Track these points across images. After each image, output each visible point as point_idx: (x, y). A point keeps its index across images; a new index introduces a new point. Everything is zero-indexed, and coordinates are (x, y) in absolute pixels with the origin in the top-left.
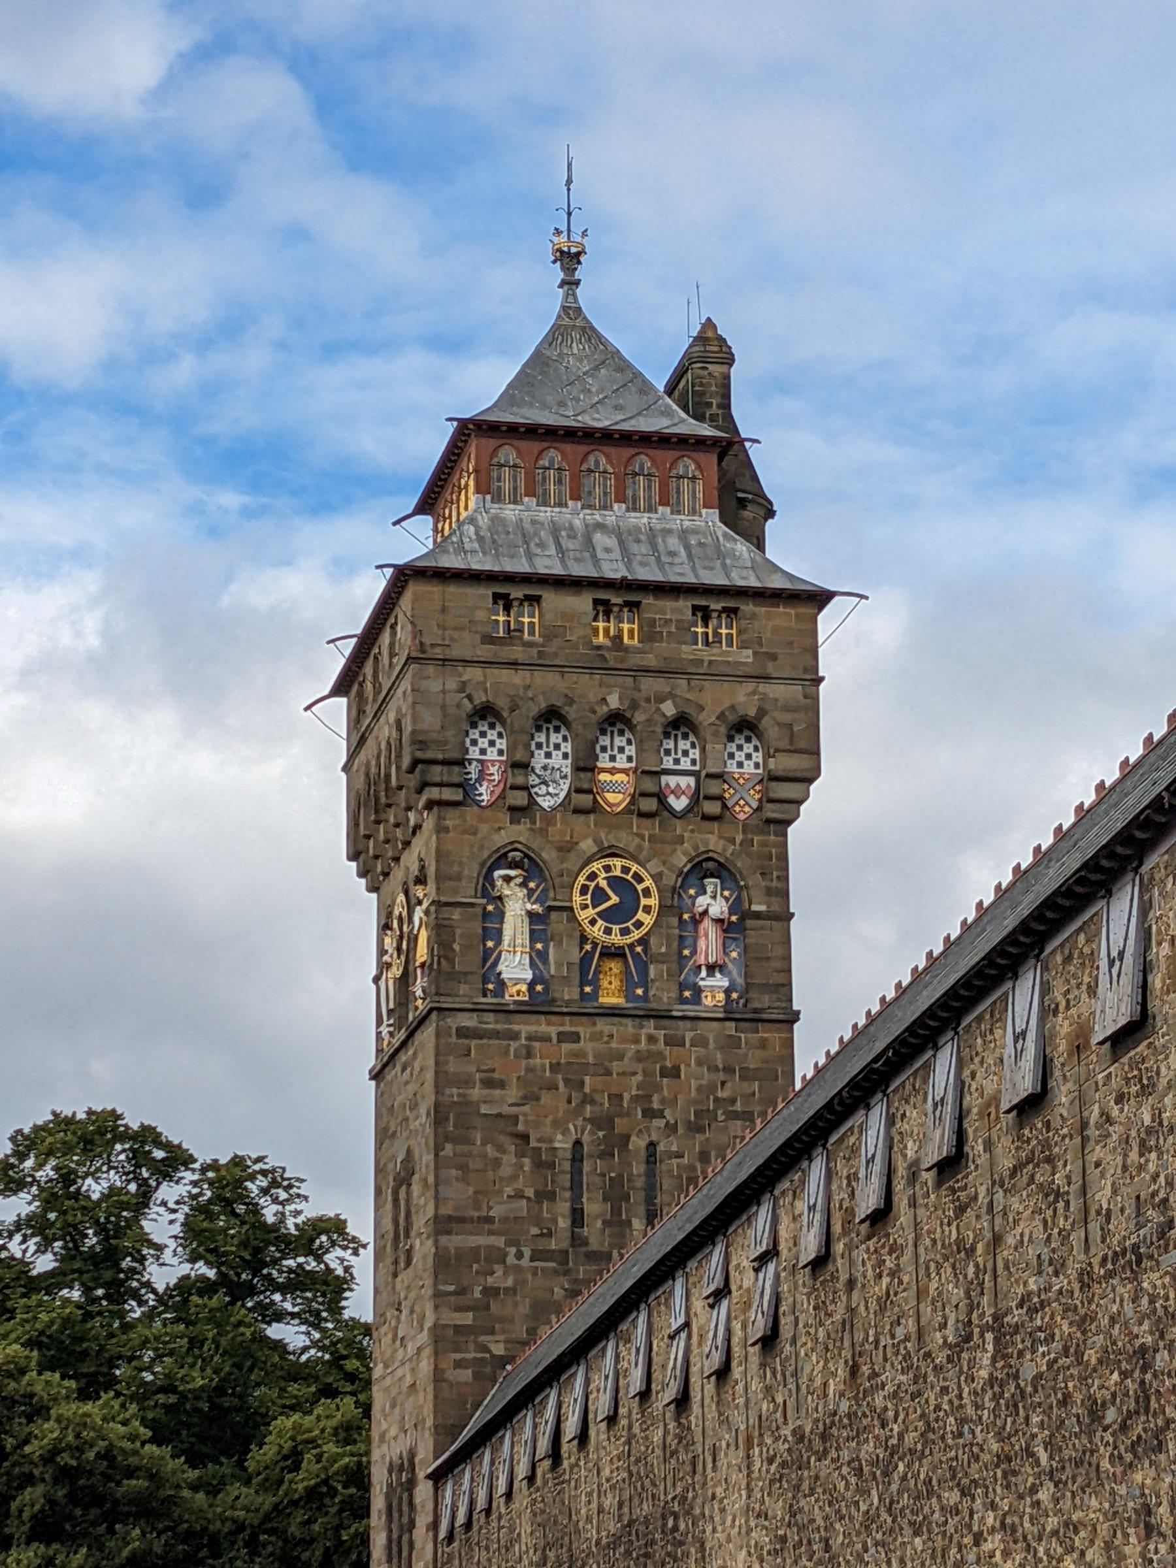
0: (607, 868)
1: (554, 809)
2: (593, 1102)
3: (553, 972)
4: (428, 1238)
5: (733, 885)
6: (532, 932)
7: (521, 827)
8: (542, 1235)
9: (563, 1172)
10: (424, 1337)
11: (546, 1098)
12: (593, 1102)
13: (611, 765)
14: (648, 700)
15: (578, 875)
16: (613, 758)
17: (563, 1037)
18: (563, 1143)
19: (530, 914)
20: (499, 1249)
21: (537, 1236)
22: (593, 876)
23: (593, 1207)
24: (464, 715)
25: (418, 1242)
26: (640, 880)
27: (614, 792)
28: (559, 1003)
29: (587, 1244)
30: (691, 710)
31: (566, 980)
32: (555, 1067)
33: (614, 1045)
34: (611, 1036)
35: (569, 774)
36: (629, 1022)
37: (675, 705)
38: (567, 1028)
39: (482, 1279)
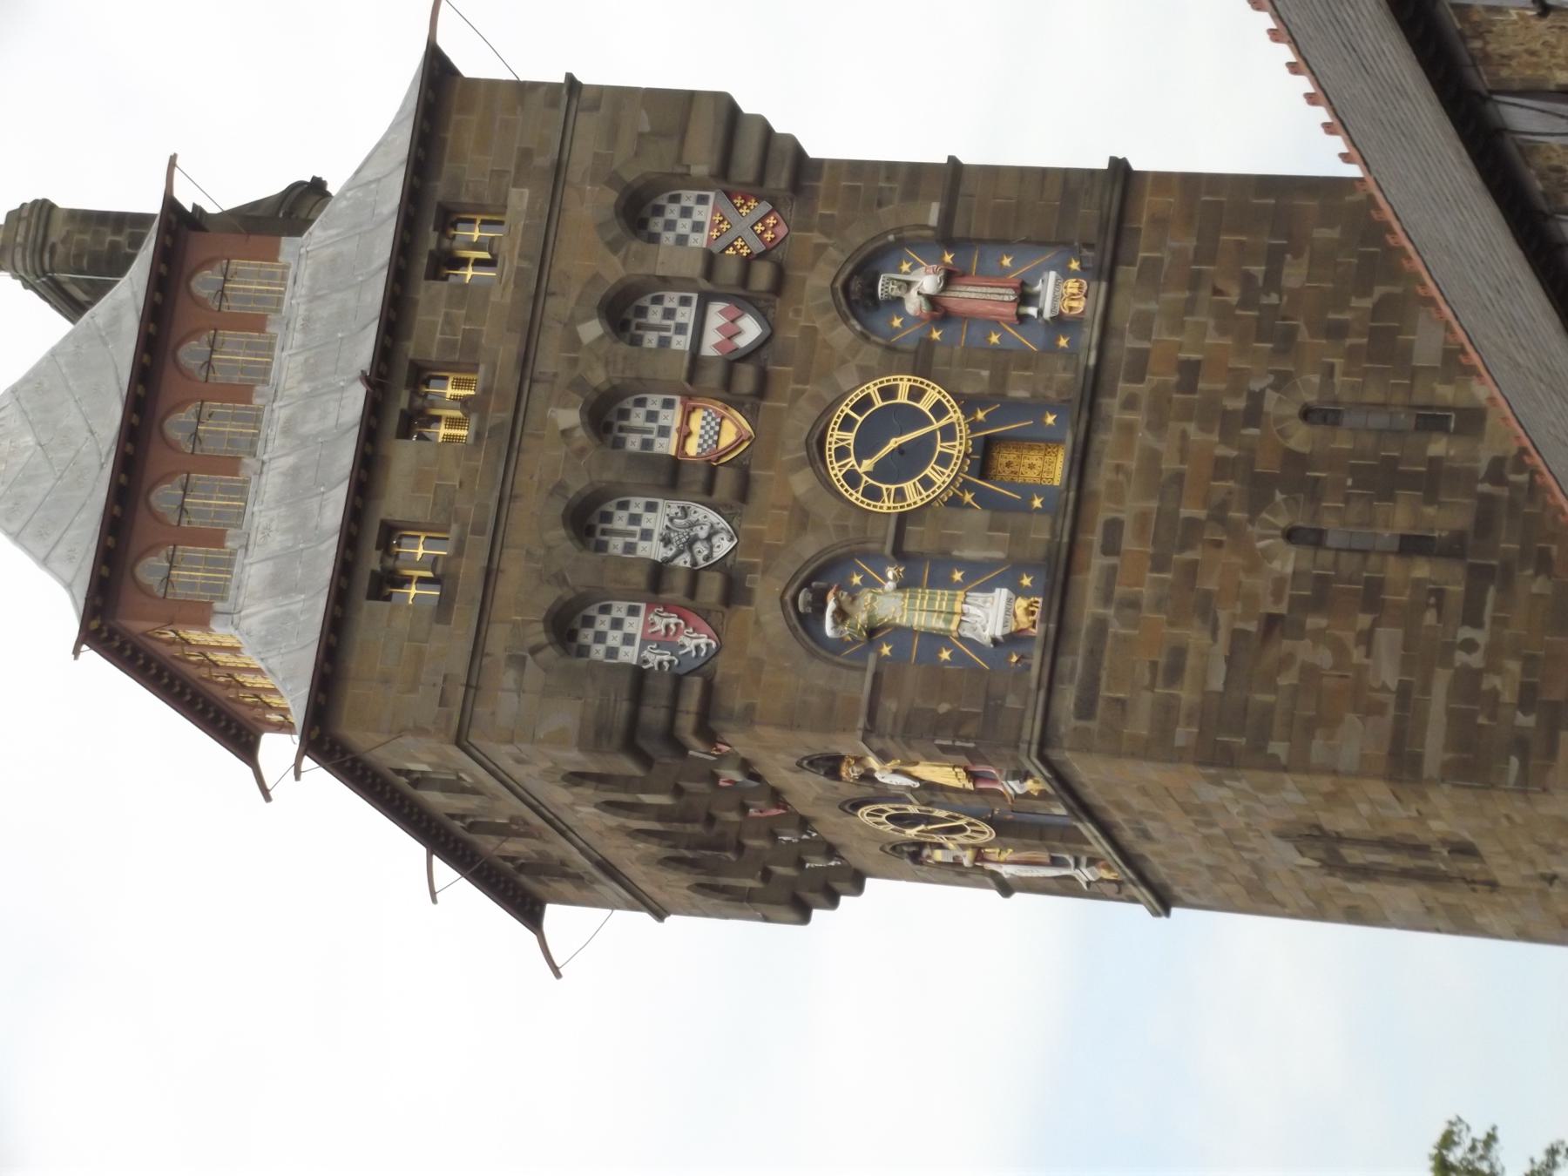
2: (1224, 506)
3: (999, 555)
4: (1424, 797)
9: (1336, 564)
11: (1210, 583)
12: (1224, 506)
13: (674, 436)
14: (574, 362)
16: (664, 431)
17: (1111, 547)
18: (1286, 561)
19: (901, 586)
23: (1401, 517)
25: (1435, 825)
26: (866, 402)
27: (718, 433)
30: (597, 296)
32: (1160, 564)
33: (1133, 464)
34: (1118, 468)
35: (682, 503)
36: (1107, 439)
37: (588, 318)
38: (1096, 538)
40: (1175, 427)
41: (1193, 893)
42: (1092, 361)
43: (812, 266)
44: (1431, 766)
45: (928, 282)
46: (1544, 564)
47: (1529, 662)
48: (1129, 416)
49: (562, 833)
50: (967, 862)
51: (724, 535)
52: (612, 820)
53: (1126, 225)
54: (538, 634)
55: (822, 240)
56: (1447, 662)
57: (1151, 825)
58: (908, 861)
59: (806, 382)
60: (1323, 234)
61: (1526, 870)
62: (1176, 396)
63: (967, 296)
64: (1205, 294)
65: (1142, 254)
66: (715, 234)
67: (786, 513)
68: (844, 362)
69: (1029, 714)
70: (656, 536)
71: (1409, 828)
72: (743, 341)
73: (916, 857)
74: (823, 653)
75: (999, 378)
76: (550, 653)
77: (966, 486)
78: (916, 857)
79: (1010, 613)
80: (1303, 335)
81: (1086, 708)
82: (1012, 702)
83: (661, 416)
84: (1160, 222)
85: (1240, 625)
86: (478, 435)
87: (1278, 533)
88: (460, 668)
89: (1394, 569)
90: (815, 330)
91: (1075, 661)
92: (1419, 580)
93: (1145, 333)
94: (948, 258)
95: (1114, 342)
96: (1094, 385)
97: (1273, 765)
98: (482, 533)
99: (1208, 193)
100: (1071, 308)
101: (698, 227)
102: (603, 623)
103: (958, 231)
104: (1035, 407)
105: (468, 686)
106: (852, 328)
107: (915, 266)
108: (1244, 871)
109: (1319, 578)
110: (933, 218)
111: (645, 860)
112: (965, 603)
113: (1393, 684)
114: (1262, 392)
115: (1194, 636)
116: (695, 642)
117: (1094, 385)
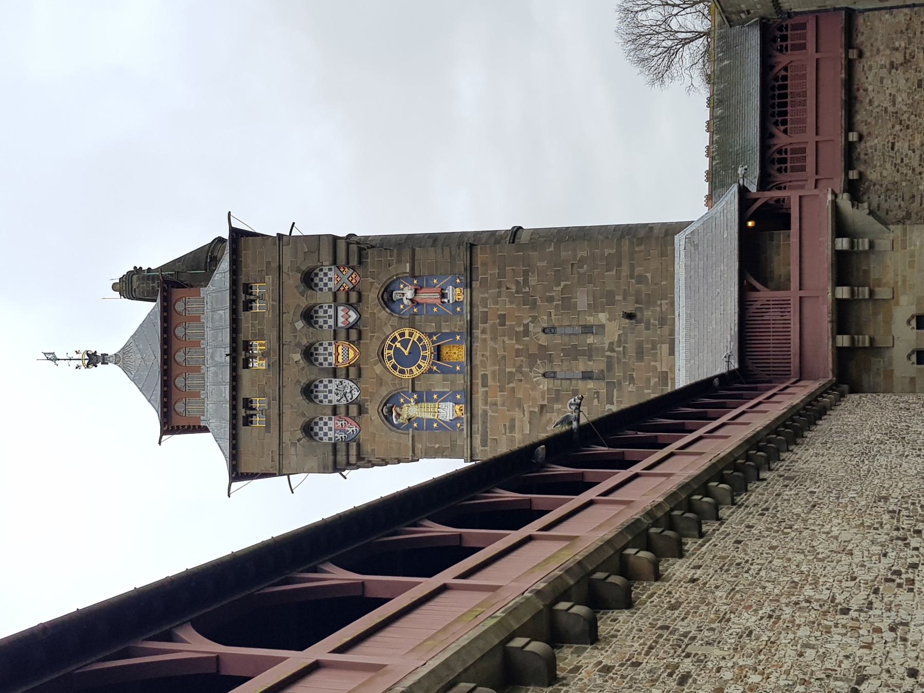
0: (390, 358)
1: (359, 389)
2: (521, 366)
5: (397, 282)
6: (427, 401)
7: (369, 407)
8: (598, 397)
9: (561, 384)
13: (334, 356)
14: (295, 337)
16: (330, 354)
17: (485, 385)
18: (545, 385)
21: (598, 401)
24: (308, 443)
27: (348, 354)
28: (465, 387)
29: (603, 371)
31: (453, 383)
35: (340, 380)
36: (477, 345)
38: (480, 381)
40: (500, 339)
42: (469, 318)
43: (370, 290)
45: (409, 294)
51: (355, 390)
53: (473, 266)
54: (299, 434)
55: (373, 281)
59: (374, 333)
62: (499, 327)
63: (423, 297)
66: (336, 282)
67: (375, 380)
68: (386, 324)
69: (465, 447)
74: (394, 429)
75: (439, 326)
77: (433, 364)
79: (454, 411)
80: (539, 302)
82: (459, 442)
83: (328, 349)
84: (484, 264)
85: (531, 410)
86: (269, 365)
87: (540, 375)
88: (276, 449)
94: (415, 282)
95: (475, 309)
96: (471, 325)
99: (500, 252)
100: (459, 299)
101: (330, 279)
102: (321, 424)
103: (417, 274)
104: (452, 334)
105: (279, 455)
106: (386, 312)
107: (405, 286)
110: (408, 270)
112: (439, 408)
114: (528, 323)
115: (517, 414)
116: (352, 429)
117: (471, 325)
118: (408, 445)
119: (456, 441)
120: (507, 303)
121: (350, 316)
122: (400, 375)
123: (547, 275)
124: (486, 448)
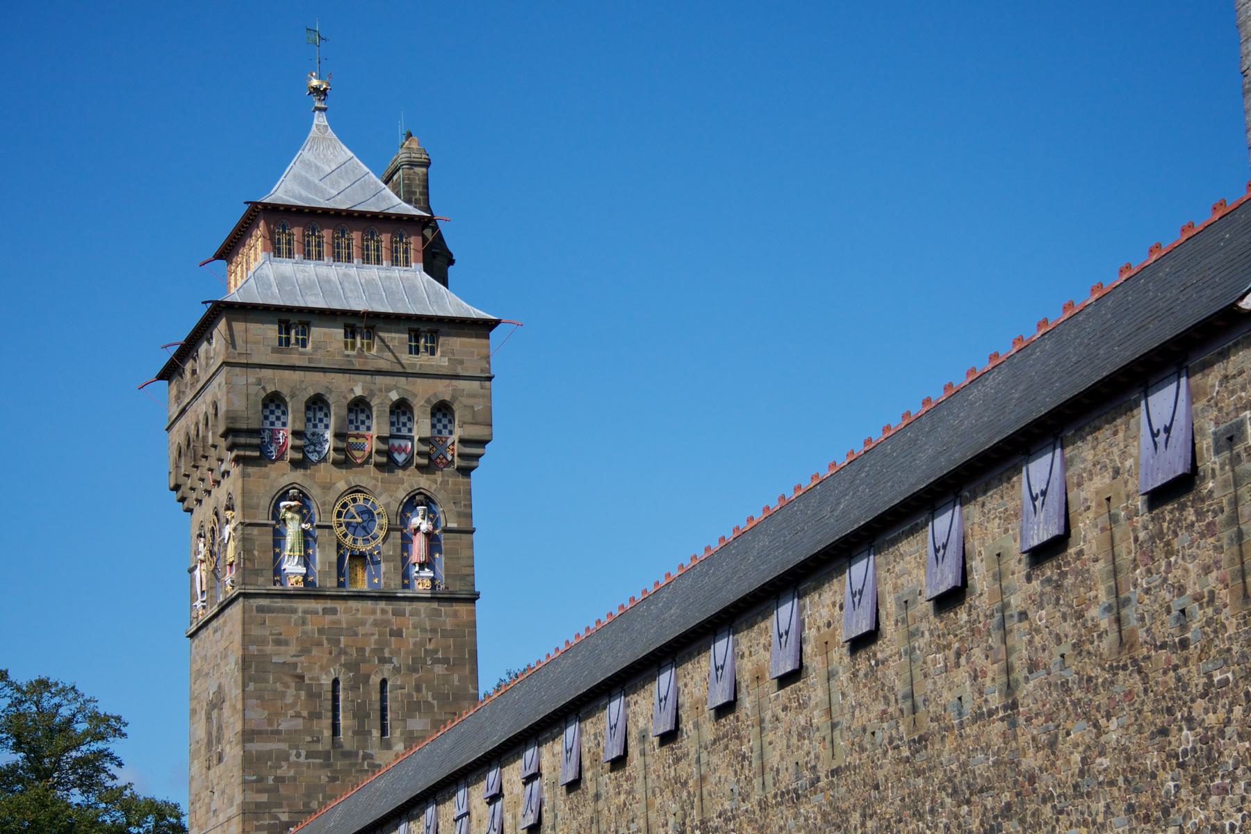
2: (346, 653)
4: (237, 744)
9: (327, 700)
10: (234, 810)
12: (346, 653)
13: (356, 432)
14: (381, 390)
15: (335, 504)
17: (325, 611)
18: (326, 681)
19: (303, 530)
20: (285, 751)
22: (345, 505)
32: (321, 631)
34: (358, 610)
37: (399, 394)
39: (273, 771)
41: (196, 648)
42: (399, 595)
44: (249, 746)
46: (333, 779)
47: (294, 779)
48: (378, 611)
49: (195, 397)
50: (199, 557)
52: (201, 418)
55: (439, 483)
56: (290, 748)
57: (219, 633)
58: (198, 533)
60: (456, 677)
61: (215, 782)
64: (429, 635)
65: (443, 609)
66: (437, 439)
68: (391, 497)
70: (315, 430)
71: (226, 737)
72: (396, 456)
73: (200, 536)
74: (274, 502)
76: (263, 395)
78: (200, 536)
79: (296, 574)
80: (415, 676)
81: (261, 609)
82: (261, 580)
84: (455, 615)
85: (299, 665)
89: (327, 722)
90: (403, 484)
91: (279, 603)
92: (321, 732)
93: (411, 615)
97: (244, 686)
98: (309, 362)
108: (206, 670)
109: (321, 693)
110: (449, 525)
111: (188, 427)
113: (280, 728)
115: (293, 648)
118: (255, 518)
119: (262, 576)
120: (414, 640)
121: (400, 454)
122: (335, 512)
123: (444, 685)
124: (255, 611)
